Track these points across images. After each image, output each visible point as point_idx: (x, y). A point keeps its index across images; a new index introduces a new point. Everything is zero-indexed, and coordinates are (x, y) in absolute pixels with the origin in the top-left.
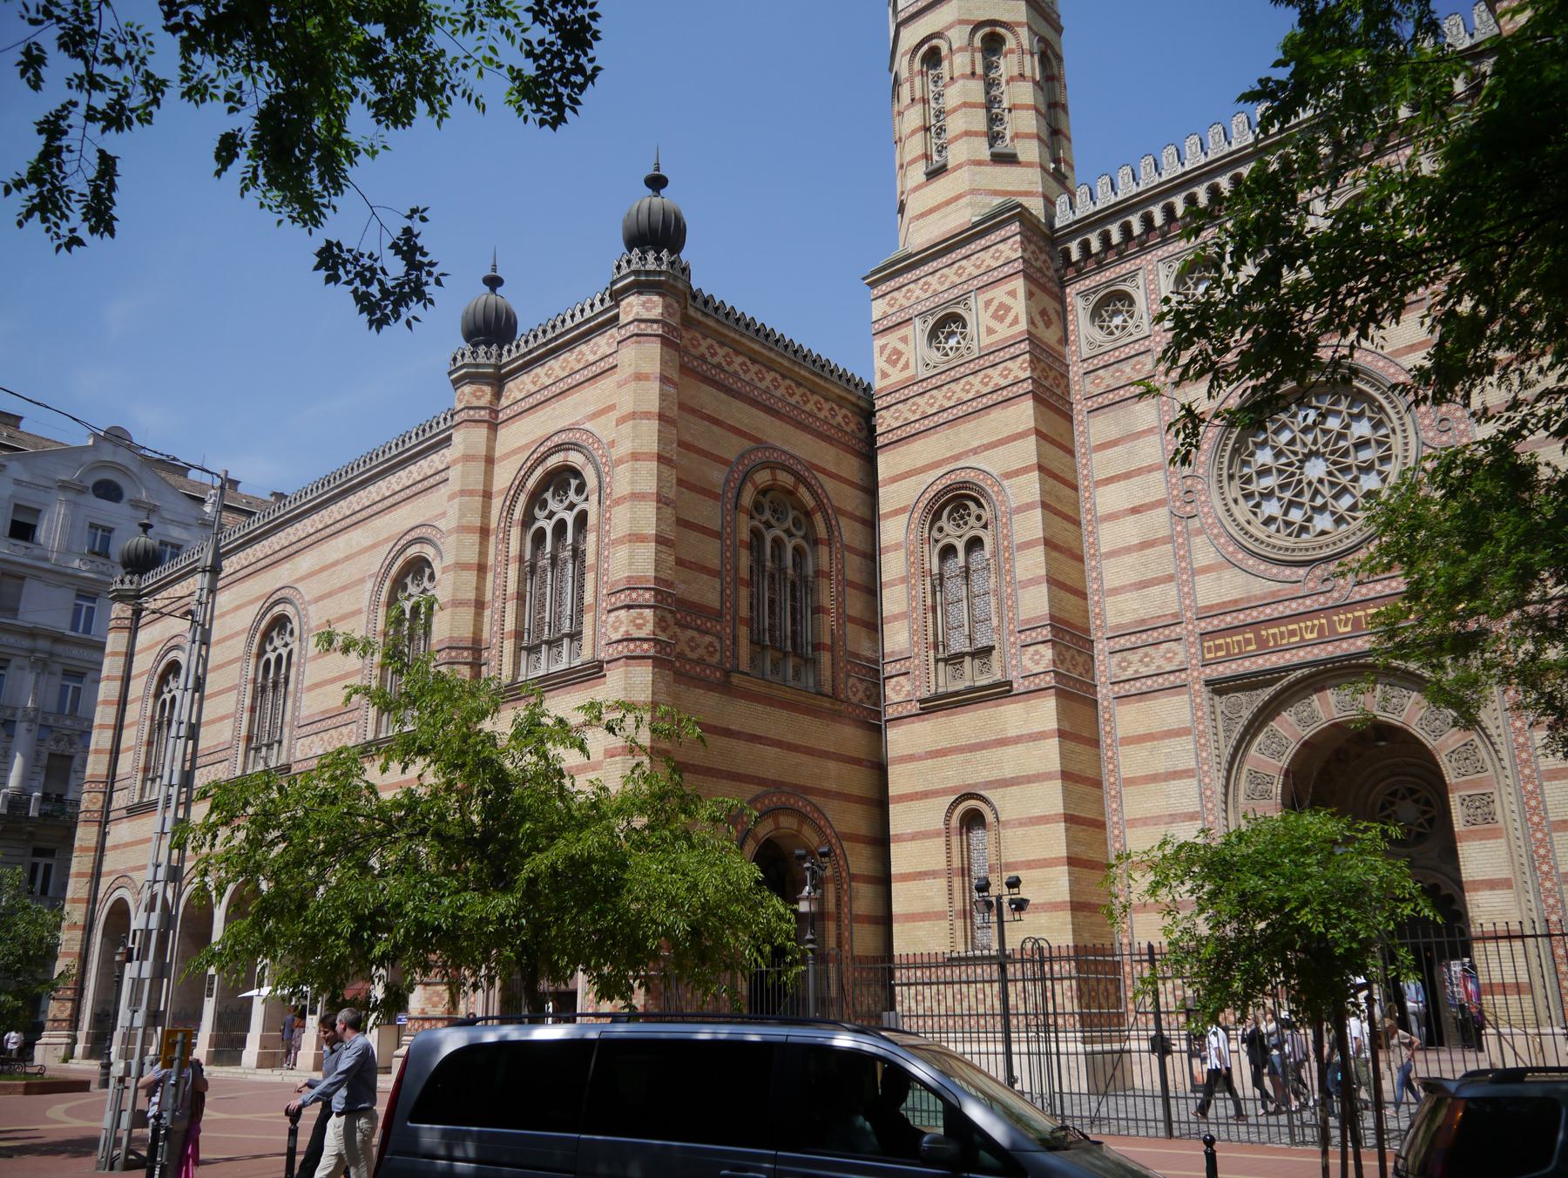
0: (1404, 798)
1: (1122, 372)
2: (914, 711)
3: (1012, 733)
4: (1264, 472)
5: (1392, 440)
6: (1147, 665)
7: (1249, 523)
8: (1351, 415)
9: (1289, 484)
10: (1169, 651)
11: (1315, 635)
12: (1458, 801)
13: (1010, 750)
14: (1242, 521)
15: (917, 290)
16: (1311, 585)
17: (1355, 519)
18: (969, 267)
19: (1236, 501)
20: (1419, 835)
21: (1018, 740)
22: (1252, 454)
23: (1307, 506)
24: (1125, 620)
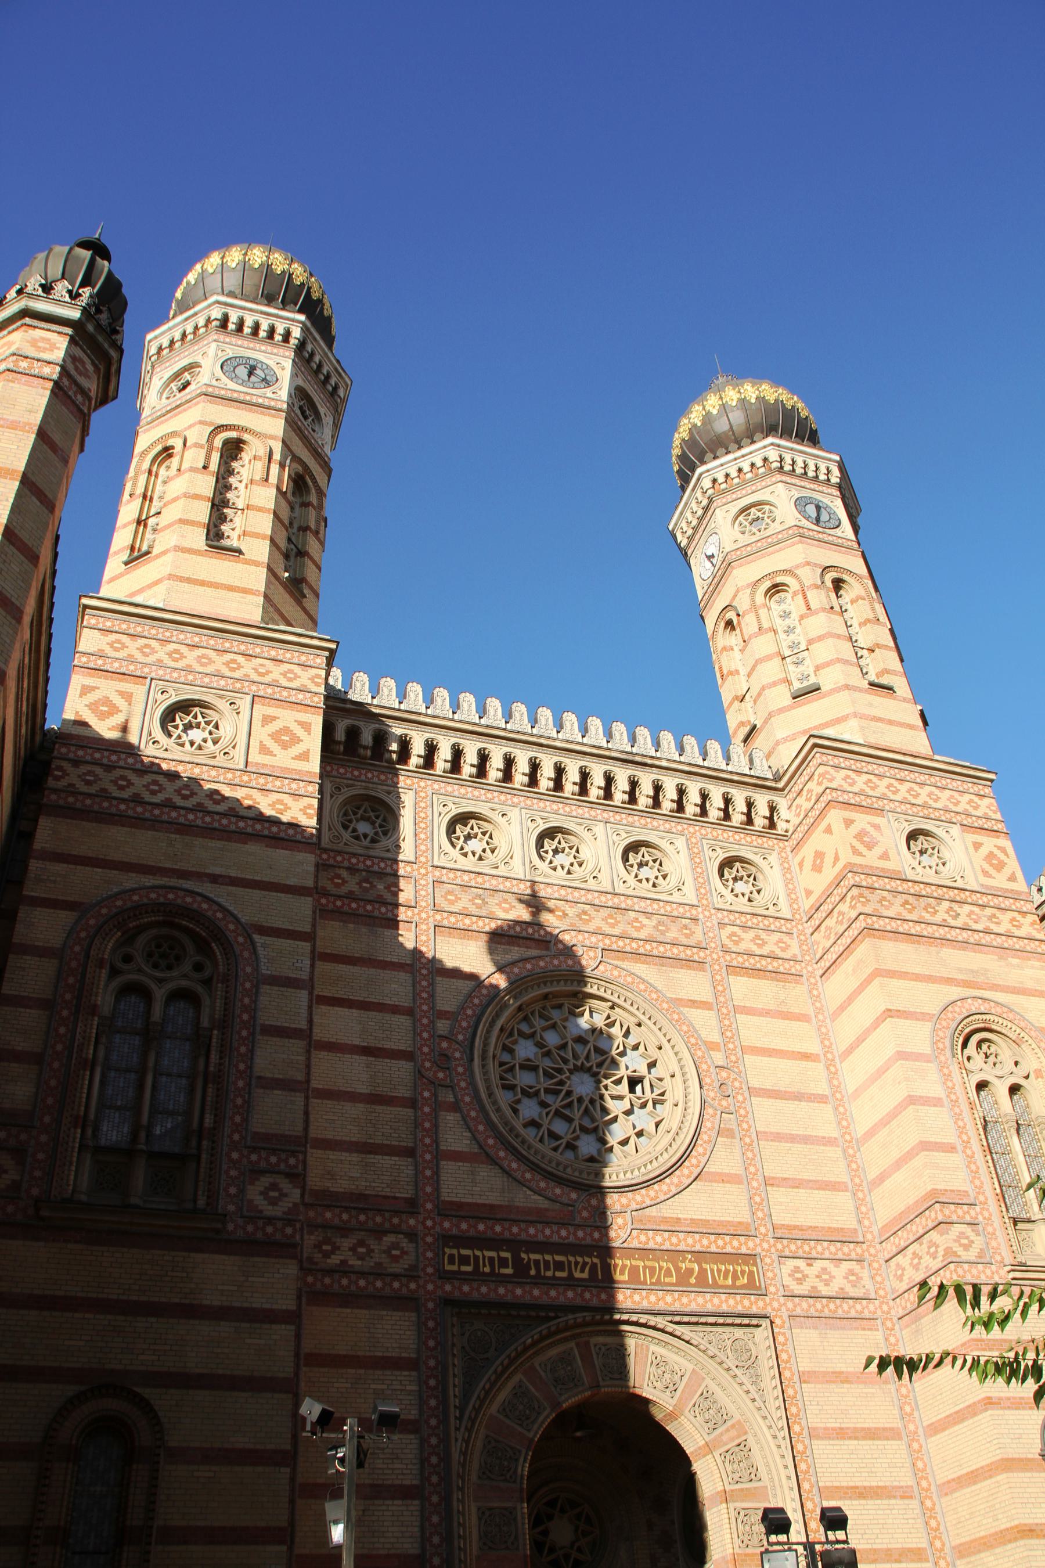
1: (373, 886)
4: (529, 1066)
6: (361, 1258)
10: (395, 1246)
12: (733, 1514)
15: (161, 653)
16: (585, 1214)
18: (247, 668)
21: (222, 1313)
22: (515, 1042)
23: (576, 1123)
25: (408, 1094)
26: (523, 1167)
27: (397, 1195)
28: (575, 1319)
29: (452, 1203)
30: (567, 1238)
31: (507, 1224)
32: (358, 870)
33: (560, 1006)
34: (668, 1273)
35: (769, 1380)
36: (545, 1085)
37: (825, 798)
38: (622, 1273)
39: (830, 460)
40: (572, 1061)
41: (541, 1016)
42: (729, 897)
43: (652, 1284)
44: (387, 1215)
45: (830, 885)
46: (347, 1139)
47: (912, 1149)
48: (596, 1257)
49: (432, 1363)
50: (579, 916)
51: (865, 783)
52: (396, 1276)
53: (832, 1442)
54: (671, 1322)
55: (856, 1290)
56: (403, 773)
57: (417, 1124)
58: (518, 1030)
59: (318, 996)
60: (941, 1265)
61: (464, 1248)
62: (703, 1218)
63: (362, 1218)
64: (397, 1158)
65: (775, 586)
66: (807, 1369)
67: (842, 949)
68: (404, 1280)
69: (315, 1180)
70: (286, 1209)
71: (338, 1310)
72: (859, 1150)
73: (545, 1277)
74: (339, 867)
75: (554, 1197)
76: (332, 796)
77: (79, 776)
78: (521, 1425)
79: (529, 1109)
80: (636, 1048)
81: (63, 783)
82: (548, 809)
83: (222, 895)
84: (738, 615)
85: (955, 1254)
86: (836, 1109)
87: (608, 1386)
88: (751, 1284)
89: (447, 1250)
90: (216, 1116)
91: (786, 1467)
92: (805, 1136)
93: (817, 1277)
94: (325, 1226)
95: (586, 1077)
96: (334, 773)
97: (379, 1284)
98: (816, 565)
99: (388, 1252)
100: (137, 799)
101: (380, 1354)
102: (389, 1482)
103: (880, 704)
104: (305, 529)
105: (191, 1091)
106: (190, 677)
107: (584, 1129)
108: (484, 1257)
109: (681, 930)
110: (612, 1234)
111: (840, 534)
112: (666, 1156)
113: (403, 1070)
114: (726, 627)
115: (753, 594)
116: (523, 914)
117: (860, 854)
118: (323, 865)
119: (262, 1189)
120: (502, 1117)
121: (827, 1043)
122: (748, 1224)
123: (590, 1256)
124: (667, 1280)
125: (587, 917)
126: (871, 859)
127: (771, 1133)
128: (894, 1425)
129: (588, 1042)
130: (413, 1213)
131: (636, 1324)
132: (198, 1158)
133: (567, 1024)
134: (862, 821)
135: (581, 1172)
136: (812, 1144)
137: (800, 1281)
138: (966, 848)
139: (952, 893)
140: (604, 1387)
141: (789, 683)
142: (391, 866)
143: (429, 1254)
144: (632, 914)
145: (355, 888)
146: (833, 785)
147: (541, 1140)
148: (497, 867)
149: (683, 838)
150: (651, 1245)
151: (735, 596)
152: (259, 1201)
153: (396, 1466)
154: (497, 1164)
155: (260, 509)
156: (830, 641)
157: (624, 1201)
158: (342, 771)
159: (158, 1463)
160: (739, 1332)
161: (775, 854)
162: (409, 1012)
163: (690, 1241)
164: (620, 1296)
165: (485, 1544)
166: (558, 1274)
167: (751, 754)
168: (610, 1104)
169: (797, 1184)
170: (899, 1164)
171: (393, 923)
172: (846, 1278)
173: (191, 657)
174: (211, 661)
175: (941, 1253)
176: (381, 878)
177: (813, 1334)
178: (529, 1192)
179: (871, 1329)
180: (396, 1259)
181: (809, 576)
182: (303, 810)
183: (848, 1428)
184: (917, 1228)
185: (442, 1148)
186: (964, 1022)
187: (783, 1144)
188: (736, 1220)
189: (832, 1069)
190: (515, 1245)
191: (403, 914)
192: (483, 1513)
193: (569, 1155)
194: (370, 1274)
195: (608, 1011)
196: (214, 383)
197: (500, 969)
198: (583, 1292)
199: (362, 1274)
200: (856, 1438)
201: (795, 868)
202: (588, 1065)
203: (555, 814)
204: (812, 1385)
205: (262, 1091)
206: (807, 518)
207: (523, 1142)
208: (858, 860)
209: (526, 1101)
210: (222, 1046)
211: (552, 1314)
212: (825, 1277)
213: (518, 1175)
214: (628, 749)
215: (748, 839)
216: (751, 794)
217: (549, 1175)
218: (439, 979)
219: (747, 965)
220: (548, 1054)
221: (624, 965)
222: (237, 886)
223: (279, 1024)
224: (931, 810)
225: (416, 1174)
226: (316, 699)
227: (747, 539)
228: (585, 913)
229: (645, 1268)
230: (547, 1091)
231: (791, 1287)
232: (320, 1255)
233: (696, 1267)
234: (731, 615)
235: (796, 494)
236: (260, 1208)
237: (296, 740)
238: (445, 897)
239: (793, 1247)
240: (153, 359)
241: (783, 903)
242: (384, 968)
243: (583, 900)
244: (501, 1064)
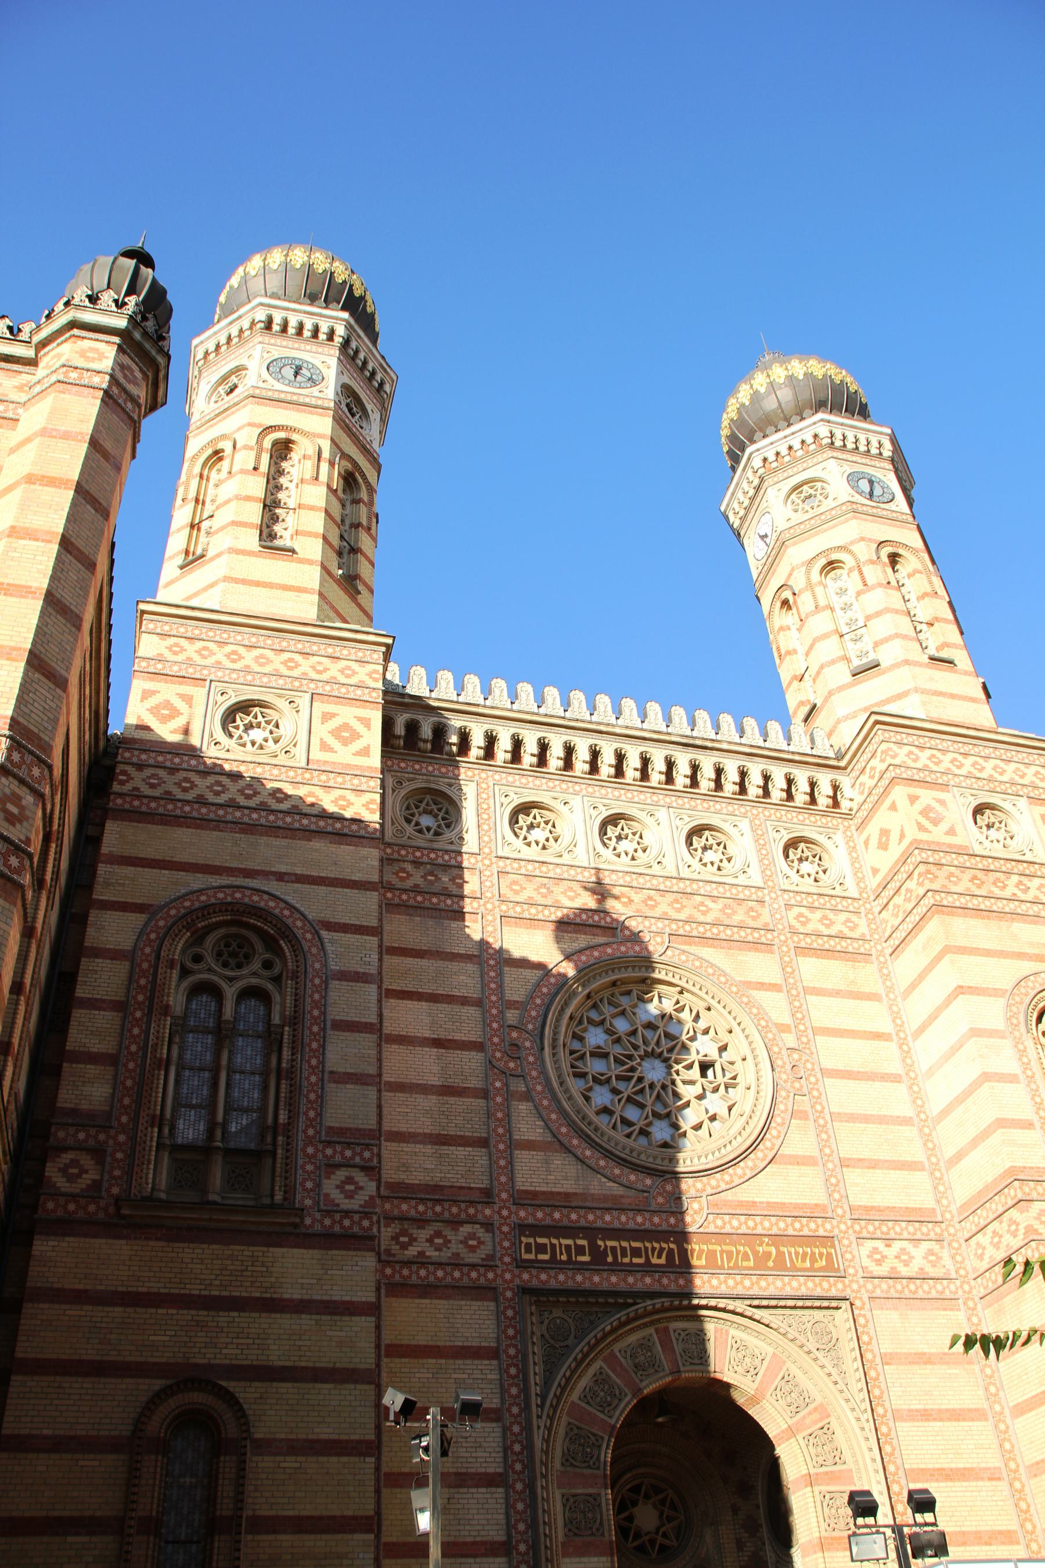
0: (647, 1497)
1: (438, 879)
2: (101, 1215)
3: (292, 1293)
4: (600, 1054)
6: (438, 1249)
10: (472, 1236)
11: (663, 1261)
13: (286, 1322)
15: (220, 654)
16: (660, 1200)
18: (305, 665)
20: (663, 1548)
22: (585, 1030)
23: (649, 1109)
25: (480, 1085)
26: (597, 1155)
27: (472, 1185)
28: (654, 1305)
29: (526, 1192)
30: (643, 1224)
31: (582, 1212)
32: (422, 863)
33: (628, 993)
34: (746, 1257)
35: (850, 1362)
36: (617, 1072)
37: (888, 775)
38: (699, 1258)
39: (881, 433)
40: (643, 1047)
42: (795, 877)
44: (463, 1205)
45: (896, 863)
46: (421, 1131)
47: (989, 1126)
49: (512, 1351)
50: (644, 902)
51: (929, 759)
52: (473, 1266)
53: (916, 1424)
54: (750, 1306)
55: (937, 1270)
56: (464, 765)
57: (489, 1115)
58: (588, 1018)
59: (387, 990)
60: (1022, 1243)
62: (779, 1200)
63: (438, 1209)
64: (470, 1149)
65: (831, 563)
66: (889, 1351)
67: (911, 926)
68: (482, 1270)
69: (390, 1173)
70: (362, 1202)
71: (417, 1301)
72: (935, 1128)
73: (622, 1264)
74: (404, 861)
75: (628, 1184)
76: (394, 791)
77: (143, 780)
78: (603, 1412)
79: (601, 1097)
80: (706, 1032)
81: (128, 787)
82: (610, 796)
83: (289, 892)
84: (794, 594)
85: (1036, 1231)
86: (911, 1088)
87: (688, 1371)
88: (830, 1266)
89: (523, 1239)
90: (290, 1111)
91: (871, 1450)
92: (880, 1116)
93: (896, 1257)
94: (402, 1219)
95: (657, 1063)
96: (396, 767)
97: (457, 1274)
98: (870, 540)
99: (464, 1242)
100: (201, 801)
101: (460, 1344)
102: (473, 1470)
103: (942, 678)
104: (357, 526)
105: (265, 1088)
106: (249, 678)
107: (656, 1115)
108: (560, 1245)
109: (747, 913)
110: (688, 1219)
111: (894, 508)
112: (739, 1139)
113: (473, 1061)
114: (782, 607)
115: (808, 572)
116: (589, 902)
117: (926, 830)
118: (387, 859)
119: (338, 1183)
120: (574, 1104)
121: (898, 1022)
123: (667, 1242)
124: (745, 1264)
125: (652, 903)
126: (937, 834)
127: (845, 1114)
128: (980, 1406)
129: (658, 1027)
130: (488, 1203)
131: (715, 1308)
132: (274, 1154)
133: (636, 1010)
134: (927, 797)
135: (655, 1158)
136: (887, 1124)
137: (879, 1262)
138: (1034, 821)
139: (1021, 867)
140: (685, 1372)
141: (849, 661)
142: (455, 858)
143: (506, 1244)
144: (699, 898)
145: (420, 881)
146: (897, 761)
147: (614, 1127)
148: (561, 856)
149: (747, 821)
150: (728, 1229)
151: (790, 575)
152: (336, 1195)
153: (480, 1454)
154: (570, 1152)
155: (312, 508)
156: (888, 616)
157: (699, 1185)
158: (403, 765)
159: (245, 1454)
160: (818, 1314)
161: (840, 834)
162: (478, 1003)
163: (766, 1224)
164: (698, 1281)
165: (570, 1530)
166: (635, 1260)
167: (812, 734)
168: (681, 1088)
169: (873, 1164)
170: (975, 1143)
171: (459, 915)
172: (925, 1258)
173: (249, 658)
174: (269, 661)
175: (1022, 1231)
176: (445, 871)
177: (894, 1315)
178: (604, 1180)
179: (952, 1310)
180: (473, 1249)
181: (864, 552)
182: (366, 806)
183: (932, 1410)
184: (997, 1206)
186: (1038, 997)
187: (857, 1125)
189: (905, 1048)
190: (591, 1232)
191: (468, 906)
192: (568, 1500)
193: (643, 1141)
194: (448, 1264)
195: (677, 996)
196: (261, 384)
197: (568, 957)
198: (660, 1278)
199: (440, 1265)
200: (941, 1420)
201: (860, 846)
202: (659, 1051)
203: (616, 801)
204: (895, 1367)
205: (334, 1085)
206: (861, 493)
207: (596, 1129)
208: (924, 836)
209: (597, 1088)
210: (294, 1042)
211: (630, 1301)
212: (904, 1257)
213: (592, 1162)
214: (688, 732)
215: (812, 819)
216: (813, 774)
217: (623, 1162)
218: (507, 969)
219: (815, 945)
220: (618, 1041)
221: (692, 949)
222: (303, 883)
223: (349, 1019)
224: (996, 784)
225: (490, 1164)
226: (374, 694)
227: (801, 517)
228: (650, 898)
229: (722, 1252)
230: (619, 1078)
231: (871, 1269)
232: (398, 1247)
233: (773, 1250)
234: (787, 594)
235: (848, 469)
236: (336, 1201)
237: (356, 736)
238: (510, 887)
239: (871, 1228)
240: (200, 364)
241: (850, 883)
242: (451, 960)
243: (648, 885)
244: (572, 1052)
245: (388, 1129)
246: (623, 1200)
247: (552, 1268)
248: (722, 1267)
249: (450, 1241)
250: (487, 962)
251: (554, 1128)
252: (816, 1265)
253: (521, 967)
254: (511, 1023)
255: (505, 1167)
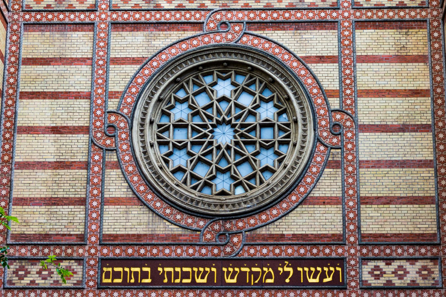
4: (180, 125)
5: (292, 130)
7: (161, 168)
8: (261, 99)
9: (202, 143)
11: (205, 281)
14: (156, 165)
16: (209, 236)
17: (251, 188)
19: (152, 146)
22: (172, 107)
23: (213, 166)
24: (30, 231)
25: (84, 159)
26: (165, 205)
27: (72, 233)
29: (110, 235)
31: (149, 248)
33: (211, 74)
36: (191, 139)
41: (195, 83)
43: (255, 284)
44: (64, 248)
46: (38, 196)
48: (214, 267)
55: (426, 281)
57: (88, 181)
58: (175, 98)
61: (117, 267)
62: (304, 233)
64: (72, 207)
73: (175, 284)
93: (393, 273)
94: (20, 259)
95: (227, 129)
108: (131, 272)
122: (340, 235)
127: (373, 161)
129: (231, 100)
136: (409, 167)
137: (377, 277)
154: (145, 205)
157: (240, 224)
162: (88, 96)
163: (290, 251)
166: (185, 281)
178: (168, 223)
185: (105, 196)
188: (331, 232)
213: (160, 212)
217: (183, 210)
218: (112, 66)
230: (193, 143)
231: (369, 282)
232: (17, 278)
233: (291, 270)
239: (376, 251)
242: (71, 64)
244: (159, 126)
245: (16, 196)
246: (181, 238)
247: (122, 289)
248: (250, 283)
249: (53, 273)
250: (97, 63)
251: (134, 188)
252: (325, 280)
253: (123, 64)
254: (110, 109)
255: (96, 219)
